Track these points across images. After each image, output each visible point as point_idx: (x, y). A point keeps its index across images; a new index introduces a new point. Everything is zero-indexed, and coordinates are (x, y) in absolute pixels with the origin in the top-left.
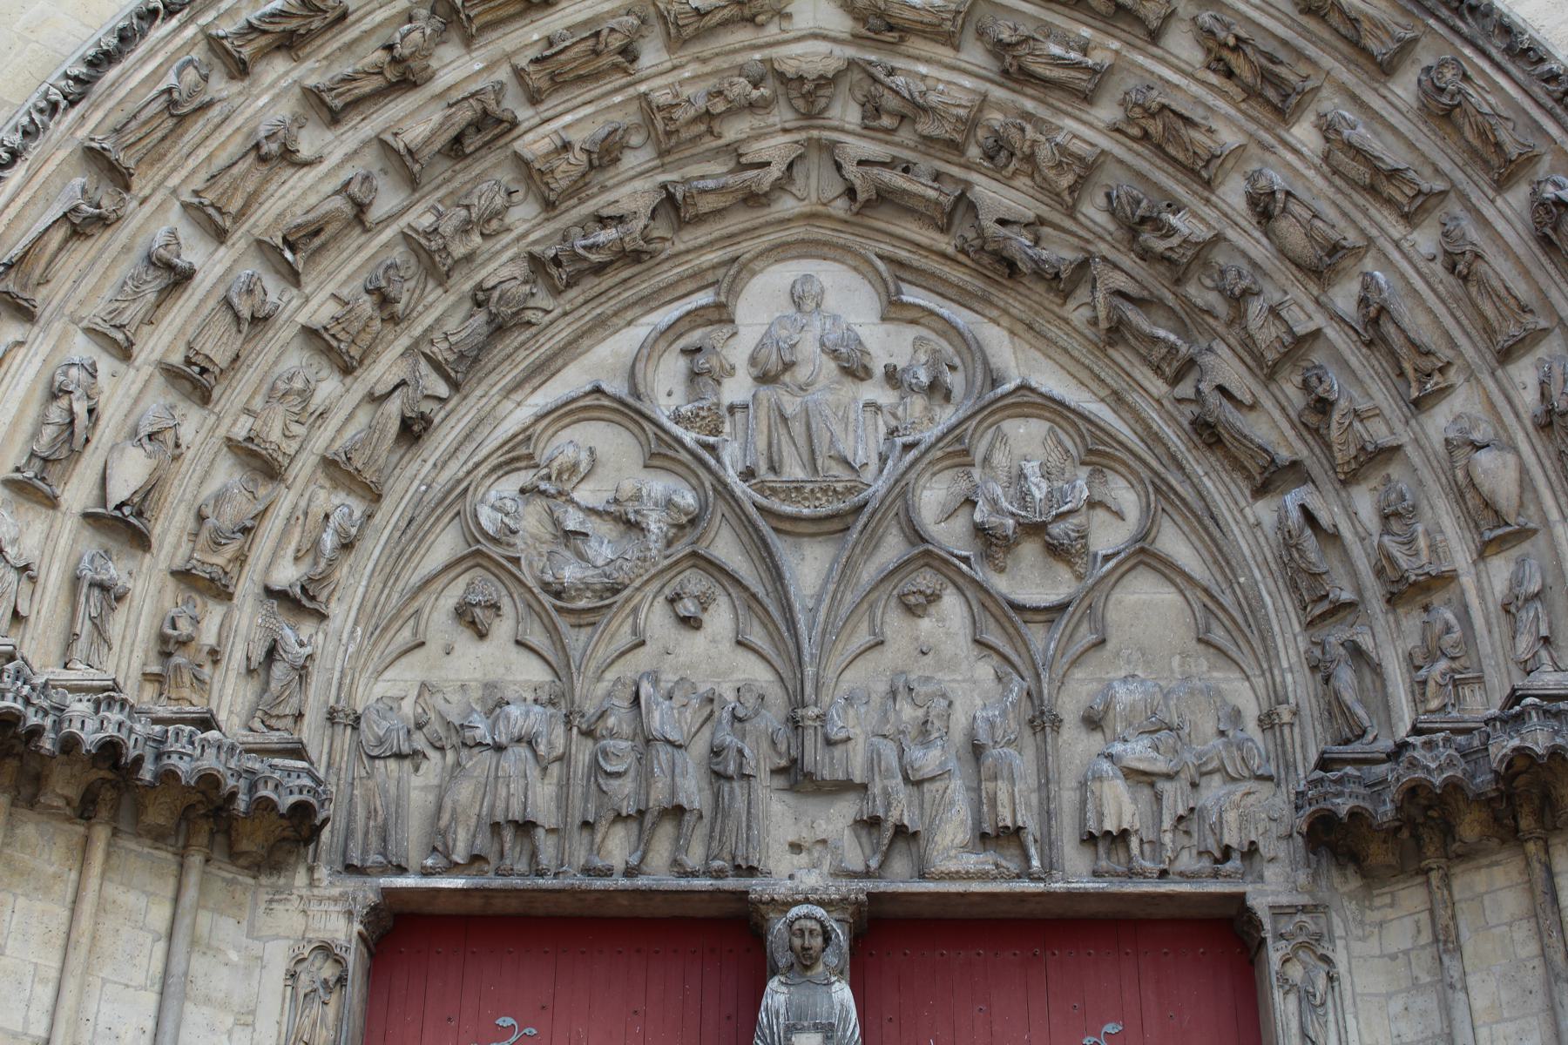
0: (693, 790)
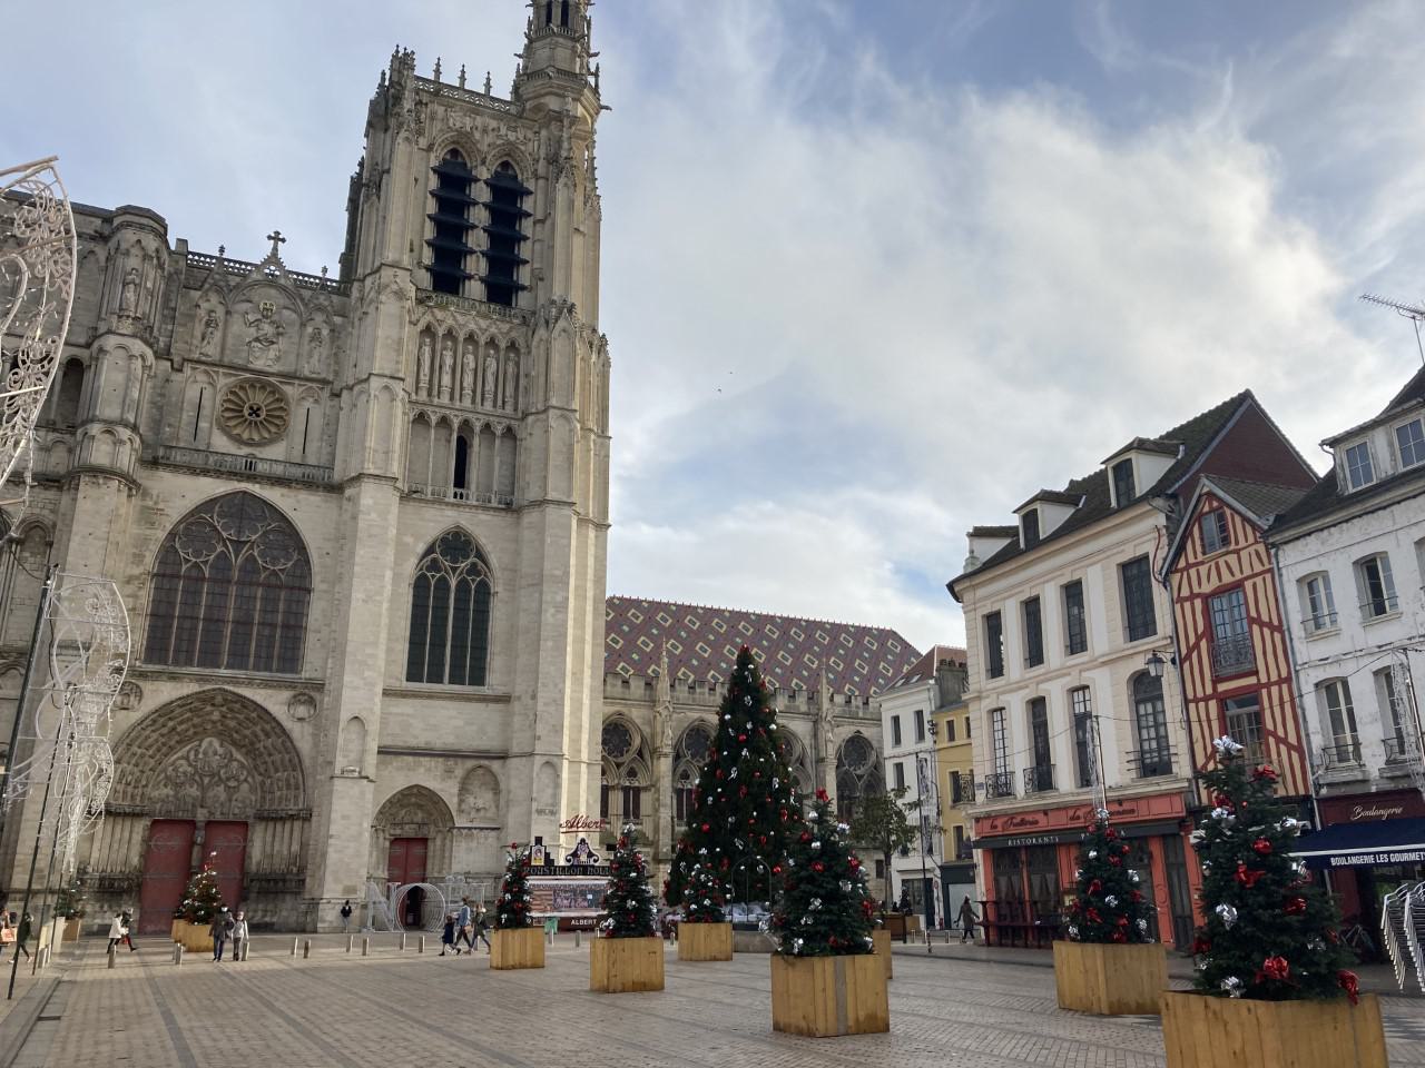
0: (190, 807)
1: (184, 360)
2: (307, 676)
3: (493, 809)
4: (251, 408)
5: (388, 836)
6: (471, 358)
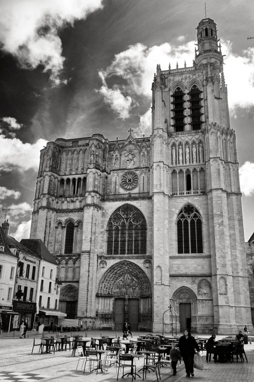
0: (124, 295)
1: (111, 171)
2: (148, 255)
3: (210, 293)
4: (129, 180)
5: (178, 302)
6: (187, 150)
